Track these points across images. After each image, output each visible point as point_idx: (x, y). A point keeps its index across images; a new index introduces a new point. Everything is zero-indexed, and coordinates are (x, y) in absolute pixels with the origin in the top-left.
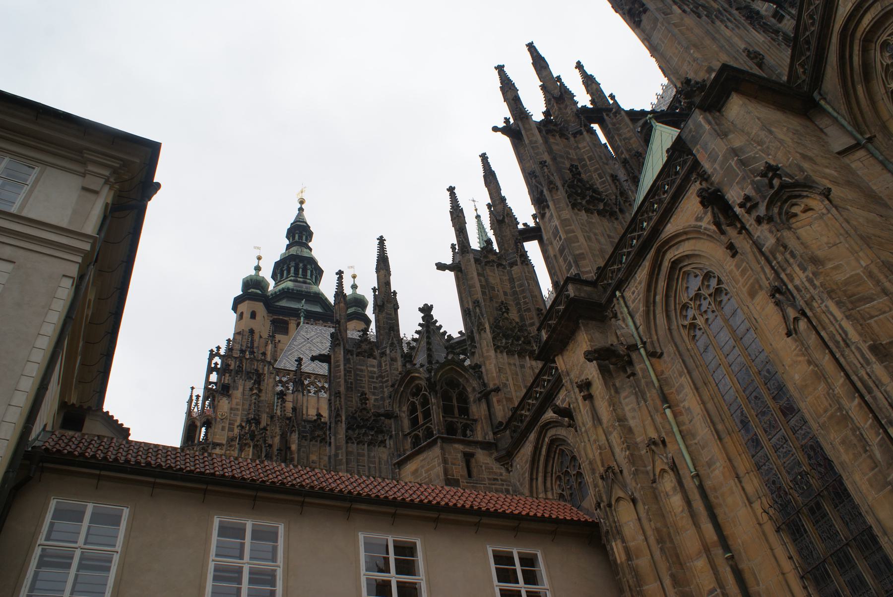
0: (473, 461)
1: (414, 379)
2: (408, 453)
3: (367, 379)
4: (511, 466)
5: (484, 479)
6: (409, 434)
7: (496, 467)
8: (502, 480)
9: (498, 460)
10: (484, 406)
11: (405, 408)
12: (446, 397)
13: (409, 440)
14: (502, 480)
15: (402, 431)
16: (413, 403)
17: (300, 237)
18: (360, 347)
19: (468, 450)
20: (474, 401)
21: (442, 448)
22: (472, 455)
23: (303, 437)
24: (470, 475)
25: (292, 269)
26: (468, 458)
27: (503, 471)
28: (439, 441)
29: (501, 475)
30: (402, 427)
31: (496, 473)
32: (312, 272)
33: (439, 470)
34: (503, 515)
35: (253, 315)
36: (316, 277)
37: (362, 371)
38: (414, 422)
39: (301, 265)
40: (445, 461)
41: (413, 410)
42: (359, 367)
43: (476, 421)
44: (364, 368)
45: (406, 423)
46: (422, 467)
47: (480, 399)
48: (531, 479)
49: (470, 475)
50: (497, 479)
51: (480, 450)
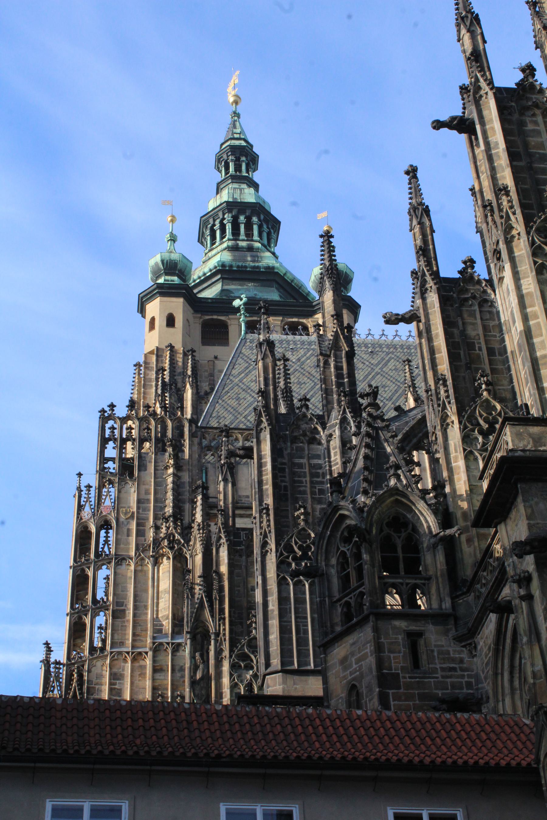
0: (422, 642)
1: (343, 517)
2: (338, 629)
3: (308, 479)
4: (475, 647)
5: (435, 671)
6: (339, 600)
7: (455, 650)
8: (462, 670)
9: (459, 639)
10: (441, 557)
11: (334, 561)
12: (387, 545)
13: (339, 610)
14: (462, 670)
15: (330, 596)
16: (343, 554)
17: (238, 168)
18: (298, 427)
19: (414, 627)
20: (429, 548)
21: (376, 630)
22: (420, 634)
23: (237, 551)
24: (416, 663)
25: (229, 227)
26: (414, 639)
27: (465, 655)
28: (372, 618)
29: (461, 661)
30: (330, 589)
31: (453, 660)
32: (260, 227)
33: (371, 660)
34: (410, 766)
35: (170, 321)
36: (269, 234)
37: (301, 466)
38: (345, 580)
39: (242, 218)
40: (379, 648)
41: (343, 564)
42: (297, 461)
43: (429, 579)
44: (304, 461)
45: (335, 582)
46: (352, 654)
47: (434, 546)
48: (496, 674)
49: (416, 663)
50: (454, 669)
51: (431, 627)
